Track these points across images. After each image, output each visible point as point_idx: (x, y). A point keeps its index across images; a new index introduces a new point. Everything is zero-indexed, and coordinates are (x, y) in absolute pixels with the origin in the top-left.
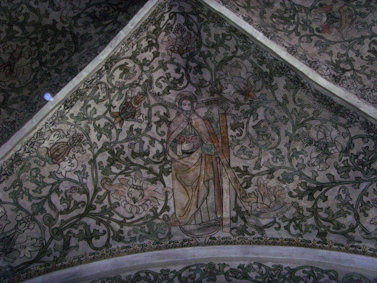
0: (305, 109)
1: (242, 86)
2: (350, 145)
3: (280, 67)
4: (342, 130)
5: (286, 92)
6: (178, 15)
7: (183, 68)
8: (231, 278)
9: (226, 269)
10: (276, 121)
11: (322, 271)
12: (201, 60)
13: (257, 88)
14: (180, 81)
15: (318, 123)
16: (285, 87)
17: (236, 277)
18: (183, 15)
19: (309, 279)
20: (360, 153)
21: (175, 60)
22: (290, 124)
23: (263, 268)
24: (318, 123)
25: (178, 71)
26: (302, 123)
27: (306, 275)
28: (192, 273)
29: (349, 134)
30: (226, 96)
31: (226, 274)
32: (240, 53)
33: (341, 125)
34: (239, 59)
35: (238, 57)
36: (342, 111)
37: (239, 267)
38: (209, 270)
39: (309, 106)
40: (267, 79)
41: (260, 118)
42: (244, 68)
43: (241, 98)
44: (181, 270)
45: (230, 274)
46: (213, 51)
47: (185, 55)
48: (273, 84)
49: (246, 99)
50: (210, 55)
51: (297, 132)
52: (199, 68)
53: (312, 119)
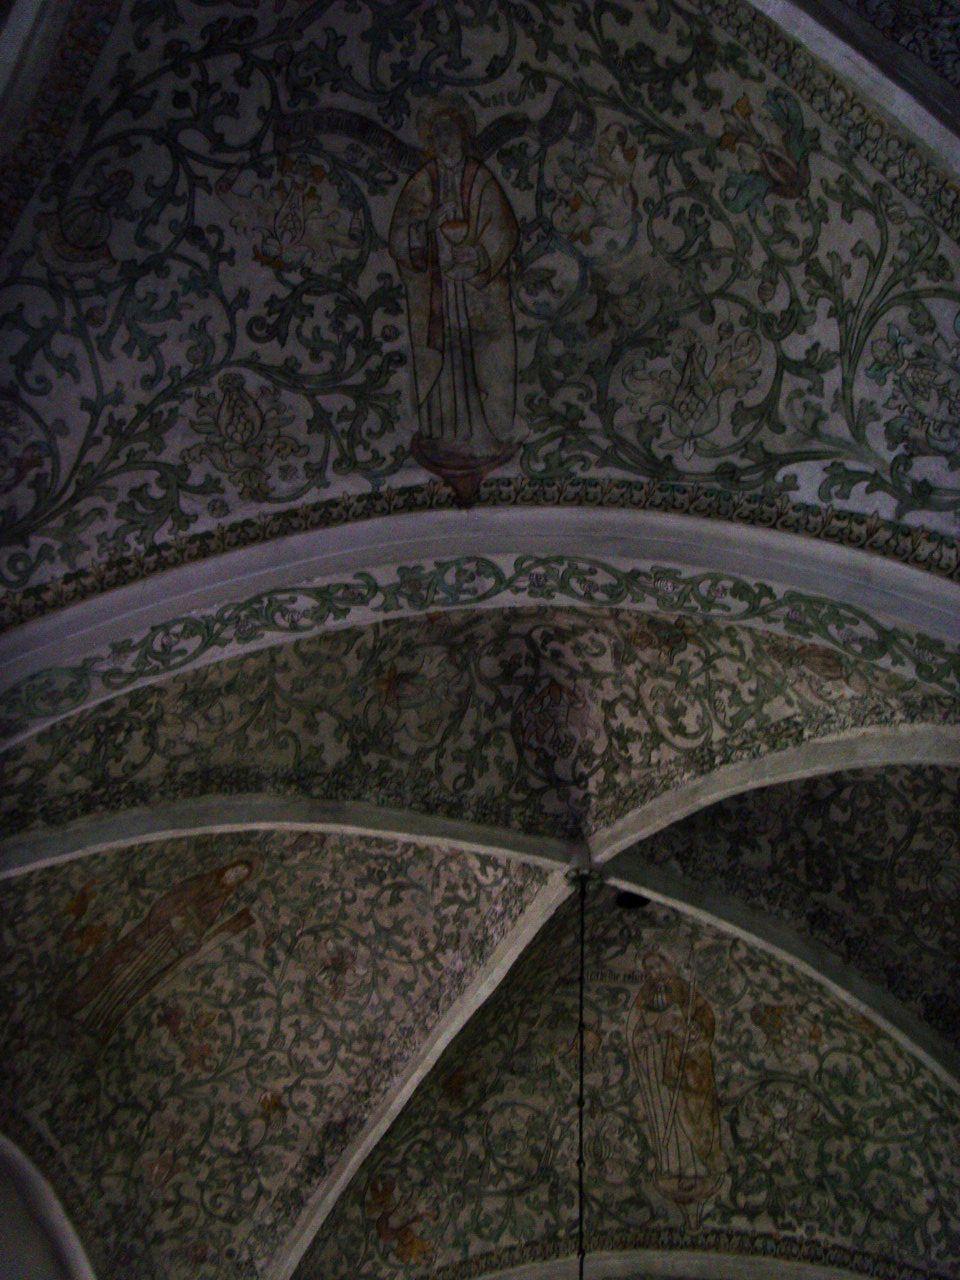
0: (265, 734)
1: (409, 690)
2: (151, 739)
3: (343, 785)
4: (181, 749)
5: (315, 740)
6: (570, 778)
7: (545, 657)
8: (359, 581)
9: (379, 599)
10: (316, 674)
11: (142, 674)
12: (506, 691)
13: (374, 706)
14: (547, 638)
15: (231, 727)
16: (320, 749)
17: (347, 587)
18: (559, 780)
19: (163, 645)
20: (126, 740)
21: (564, 672)
22: (286, 686)
23: (283, 623)
24: (231, 727)
25: (556, 654)
26: (261, 703)
27: (174, 649)
28: (465, 586)
29: (163, 753)
30: (438, 649)
31: (375, 588)
32: (430, 763)
33: (186, 756)
34: (429, 745)
35: (431, 750)
36: (198, 783)
37: (347, 611)
38: (424, 593)
39: (261, 745)
40: (360, 738)
41: (352, 654)
42: (413, 731)
43: (403, 665)
44: (498, 592)
45: (365, 592)
46: (486, 725)
47: (545, 683)
48: (346, 738)
49: (394, 668)
50: (490, 713)
51: (265, 682)
52: (508, 671)
53: (245, 726)
